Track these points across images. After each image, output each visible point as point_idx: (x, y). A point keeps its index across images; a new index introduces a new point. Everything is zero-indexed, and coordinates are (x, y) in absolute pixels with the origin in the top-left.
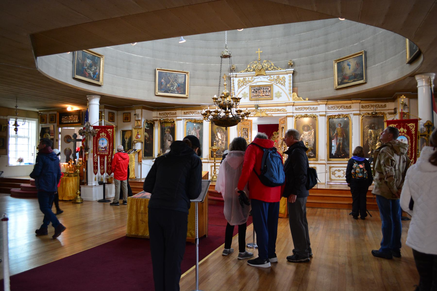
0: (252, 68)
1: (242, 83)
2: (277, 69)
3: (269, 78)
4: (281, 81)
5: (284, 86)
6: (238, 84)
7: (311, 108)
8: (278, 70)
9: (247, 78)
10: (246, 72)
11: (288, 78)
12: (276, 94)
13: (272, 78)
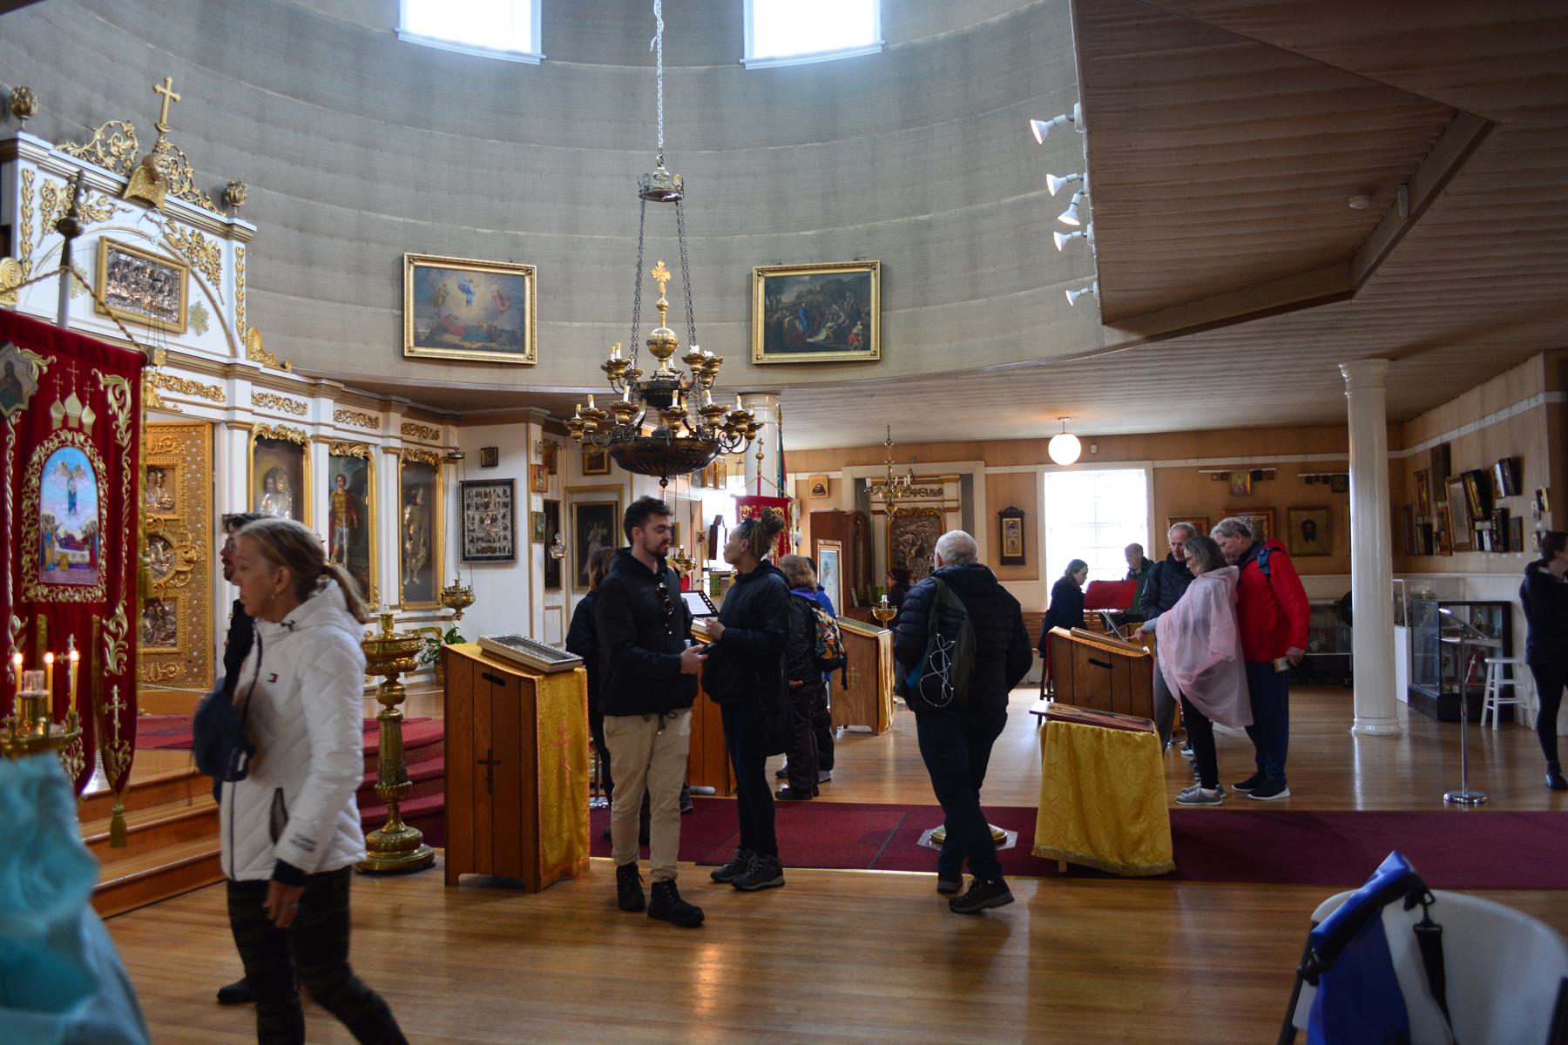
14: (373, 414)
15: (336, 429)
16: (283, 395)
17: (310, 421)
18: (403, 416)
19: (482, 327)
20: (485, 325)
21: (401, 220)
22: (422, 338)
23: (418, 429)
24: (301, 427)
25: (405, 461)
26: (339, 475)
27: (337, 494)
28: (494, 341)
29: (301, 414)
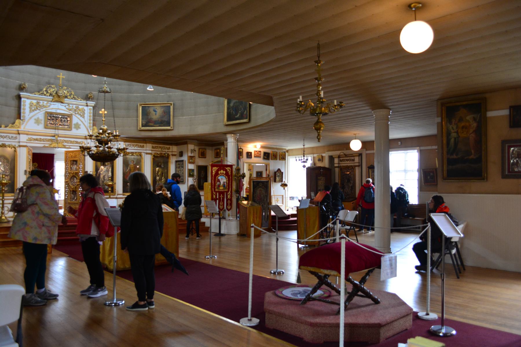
0: (49, 92)
1: (35, 107)
2: (77, 98)
3: (67, 107)
4: (80, 112)
5: (84, 117)
6: (30, 108)
8: (78, 100)
9: (41, 102)
10: (42, 95)
11: (88, 111)
12: (75, 124)
13: (70, 107)
14: (142, 144)
18: (152, 144)
19: (159, 120)
20: (160, 120)
21: (139, 95)
22: (144, 125)
23: (160, 147)
25: (154, 156)
28: (162, 124)
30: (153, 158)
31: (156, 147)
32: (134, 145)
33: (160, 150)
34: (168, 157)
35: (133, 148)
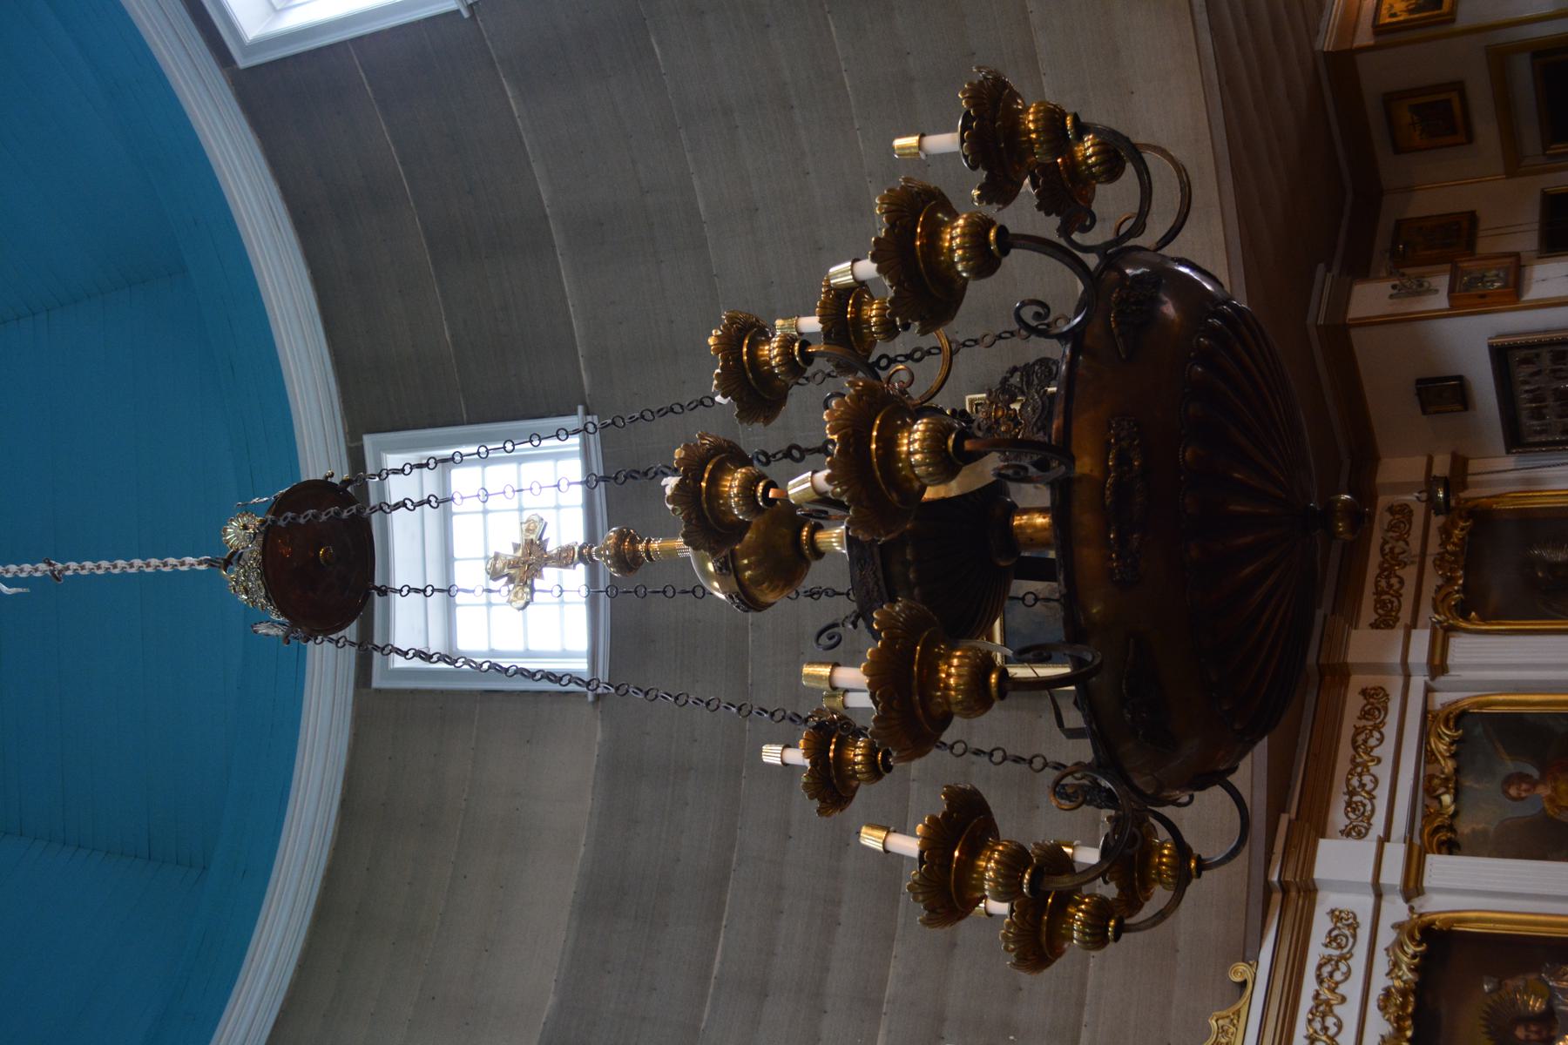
7: (1329, 960)
14: (1354, 703)
15: (1385, 838)
16: (1309, 985)
17: (1370, 900)
18: (1353, 622)
23: (1386, 571)
24: (1386, 937)
25: (1463, 611)
26: (1506, 792)
27: (1551, 800)
29: (1354, 927)
30: (1484, 618)
31: (1380, 604)
32: (1353, 760)
33: (1409, 574)
34: (1483, 519)
35: (1383, 772)
